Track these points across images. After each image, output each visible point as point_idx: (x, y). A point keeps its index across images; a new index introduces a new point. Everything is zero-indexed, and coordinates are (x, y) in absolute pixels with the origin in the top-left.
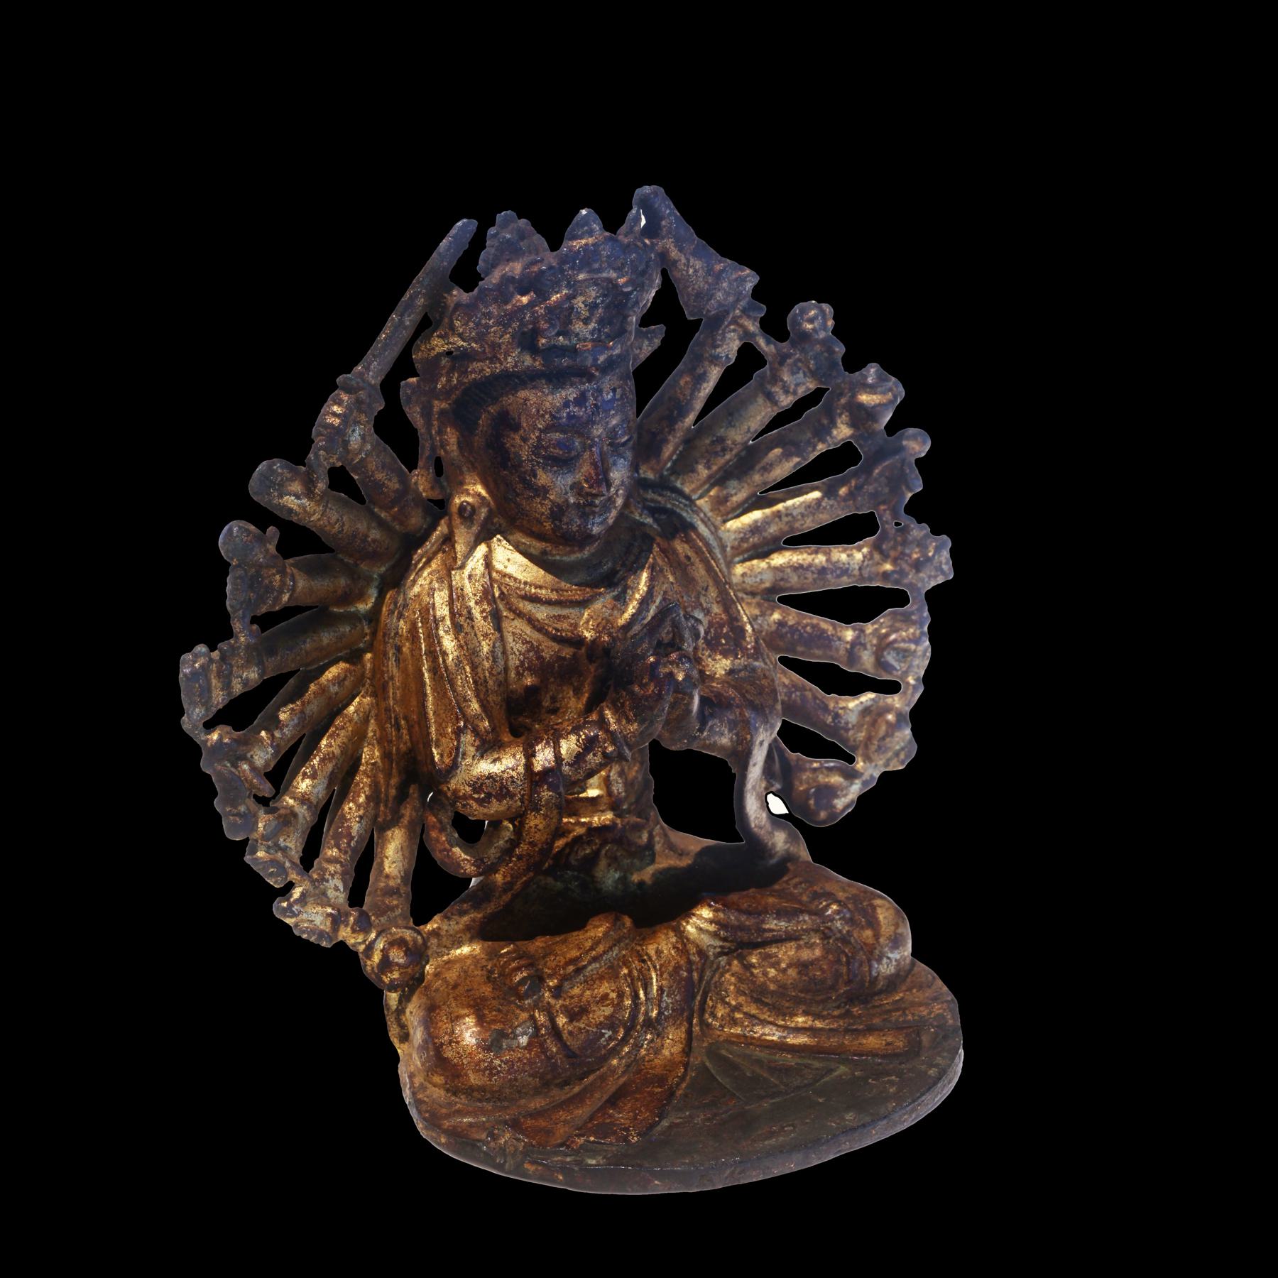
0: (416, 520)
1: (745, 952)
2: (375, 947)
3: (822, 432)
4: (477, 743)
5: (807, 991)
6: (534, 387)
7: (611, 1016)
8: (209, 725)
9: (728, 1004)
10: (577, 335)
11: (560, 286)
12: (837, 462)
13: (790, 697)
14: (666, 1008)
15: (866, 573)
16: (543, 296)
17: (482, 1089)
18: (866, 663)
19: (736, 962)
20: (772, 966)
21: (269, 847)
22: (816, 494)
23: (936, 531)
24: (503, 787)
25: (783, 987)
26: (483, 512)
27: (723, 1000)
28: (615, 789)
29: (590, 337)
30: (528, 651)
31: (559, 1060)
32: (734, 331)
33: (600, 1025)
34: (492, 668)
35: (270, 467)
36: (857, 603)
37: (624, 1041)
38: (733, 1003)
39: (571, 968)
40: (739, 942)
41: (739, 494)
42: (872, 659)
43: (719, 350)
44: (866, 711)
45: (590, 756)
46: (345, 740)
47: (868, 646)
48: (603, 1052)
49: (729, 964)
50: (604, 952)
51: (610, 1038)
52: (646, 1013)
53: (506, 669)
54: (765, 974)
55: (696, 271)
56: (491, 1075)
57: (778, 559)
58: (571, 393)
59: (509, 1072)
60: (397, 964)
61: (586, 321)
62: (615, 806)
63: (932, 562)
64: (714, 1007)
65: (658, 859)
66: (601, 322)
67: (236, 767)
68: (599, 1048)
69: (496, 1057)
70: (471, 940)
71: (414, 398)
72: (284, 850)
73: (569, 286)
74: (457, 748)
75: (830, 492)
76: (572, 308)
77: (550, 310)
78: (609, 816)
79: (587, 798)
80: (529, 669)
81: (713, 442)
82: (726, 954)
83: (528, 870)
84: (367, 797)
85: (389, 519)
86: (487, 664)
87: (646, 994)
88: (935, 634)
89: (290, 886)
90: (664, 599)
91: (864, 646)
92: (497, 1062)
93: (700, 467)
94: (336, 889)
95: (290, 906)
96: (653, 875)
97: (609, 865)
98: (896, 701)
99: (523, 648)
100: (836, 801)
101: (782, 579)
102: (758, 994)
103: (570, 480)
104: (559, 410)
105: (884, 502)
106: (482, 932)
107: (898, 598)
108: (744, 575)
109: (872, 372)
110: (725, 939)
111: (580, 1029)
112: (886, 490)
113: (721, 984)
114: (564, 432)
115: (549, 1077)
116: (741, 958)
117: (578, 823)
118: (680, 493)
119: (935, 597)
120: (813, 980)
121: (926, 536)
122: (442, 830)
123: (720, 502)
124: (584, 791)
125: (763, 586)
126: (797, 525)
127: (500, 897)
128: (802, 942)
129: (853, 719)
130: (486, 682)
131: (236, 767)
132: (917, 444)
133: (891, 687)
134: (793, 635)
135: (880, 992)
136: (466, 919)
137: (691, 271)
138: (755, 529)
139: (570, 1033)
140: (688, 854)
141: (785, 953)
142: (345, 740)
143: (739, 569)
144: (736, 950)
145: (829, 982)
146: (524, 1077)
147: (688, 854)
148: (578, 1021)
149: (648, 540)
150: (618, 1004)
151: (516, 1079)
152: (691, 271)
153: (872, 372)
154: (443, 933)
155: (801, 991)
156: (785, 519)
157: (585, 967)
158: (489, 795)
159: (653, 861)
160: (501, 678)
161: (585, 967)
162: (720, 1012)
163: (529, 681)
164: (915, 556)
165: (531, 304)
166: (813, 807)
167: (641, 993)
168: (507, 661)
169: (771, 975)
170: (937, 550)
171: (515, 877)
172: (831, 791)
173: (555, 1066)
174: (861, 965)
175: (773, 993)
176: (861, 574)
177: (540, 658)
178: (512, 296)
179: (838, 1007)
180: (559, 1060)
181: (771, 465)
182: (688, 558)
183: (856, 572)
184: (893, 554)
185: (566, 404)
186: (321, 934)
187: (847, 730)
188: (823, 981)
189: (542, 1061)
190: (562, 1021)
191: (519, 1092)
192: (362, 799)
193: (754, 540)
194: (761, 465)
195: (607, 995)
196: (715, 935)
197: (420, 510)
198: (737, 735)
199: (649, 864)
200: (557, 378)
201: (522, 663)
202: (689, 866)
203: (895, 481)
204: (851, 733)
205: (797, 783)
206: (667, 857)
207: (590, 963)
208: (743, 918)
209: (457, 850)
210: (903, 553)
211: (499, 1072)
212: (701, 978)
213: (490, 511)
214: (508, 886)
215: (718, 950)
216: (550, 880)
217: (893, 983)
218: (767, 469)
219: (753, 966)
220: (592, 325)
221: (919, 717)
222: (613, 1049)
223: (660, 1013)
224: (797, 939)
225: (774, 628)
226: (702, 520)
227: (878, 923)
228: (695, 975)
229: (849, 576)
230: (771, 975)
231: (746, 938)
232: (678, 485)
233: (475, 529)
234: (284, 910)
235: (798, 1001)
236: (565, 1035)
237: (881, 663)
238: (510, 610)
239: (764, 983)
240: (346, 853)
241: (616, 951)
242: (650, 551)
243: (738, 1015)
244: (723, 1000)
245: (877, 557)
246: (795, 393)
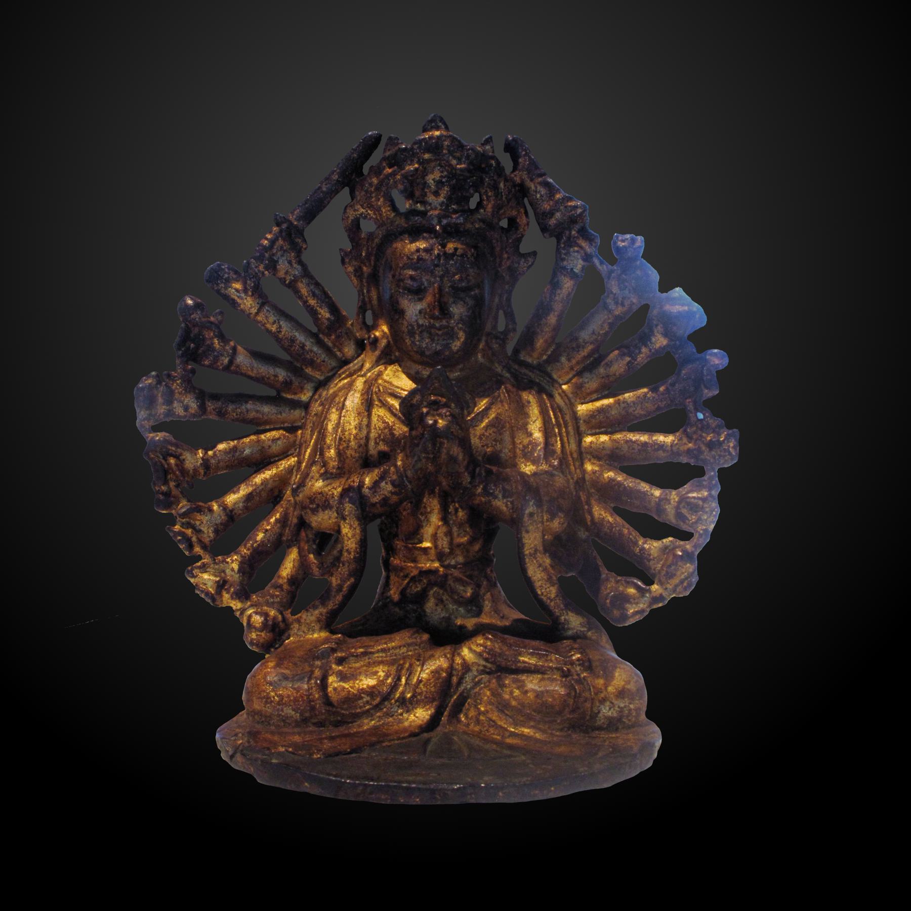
0: (349, 350)
1: (503, 675)
2: (253, 616)
3: (645, 339)
4: (322, 471)
5: (539, 712)
6: (402, 240)
7: (374, 687)
8: (155, 429)
9: (479, 709)
10: (430, 204)
11: (412, 161)
12: (660, 369)
13: (611, 530)
14: (420, 694)
15: (675, 449)
16: (401, 168)
17: (259, 713)
18: (670, 516)
19: (494, 681)
20: (518, 688)
21: (183, 524)
22: (645, 390)
23: (729, 427)
24: (327, 500)
25: (523, 705)
26: (383, 343)
27: (476, 706)
28: (440, 543)
29: (439, 207)
30: (385, 428)
31: (318, 705)
32: (577, 252)
33: (362, 691)
34: (357, 434)
35: (219, 266)
36: (672, 474)
37: (377, 707)
38: (482, 709)
39: (361, 650)
40: (500, 668)
41: (592, 383)
42: (673, 512)
43: (565, 263)
44: (665, 549)
45: (383, 484)
46: (268, 477)
47: (672, 502)
48: (359, 710)
49: (489, 681)
50: (393, 648)
51: (367, 702)
52: (403, 693)
53: (367, 438)
54: (511, 693)
55: (541, 196)
56: (266, 702)
57: (618, 436)
58: (422, 245)
59: (279, 703)
60: (255, 627)
61: (436, 194)
62: (440, 557)
63: (727, 449)
64: (468, 710)
65: (483, 615)
66: (449, 199)
67: (166, 460)
68: (356, 707)
69: (273, 690)
70: (321, 629)
71: (347, 260)
72: (198, 531)
73: (418, 162)
74: (308, 475)
75: (654, 390)
76: (425, 183)
77: (405, 177)
78: (436, 565)
79: (421, 548)
80: (383, 440)
81: (571, 341)
82: (488, 673)
83: (350, 575)
84: (276, 519)
85: (330, 344)
86: (354, 432)
87: (407, 680)
88: (721, 499)
89: (199, 558)
90: (496, 418)
91: (668, 501)
92: (273, 694)
93: (563, 359)
94: (233, 570)
95: (192, 570)
96: (475, 625)
97: (437, 605)
98: (688, 546)
99: (382, 426)
100: (628, 605)
101: (617, 448)
102: (503, 707)
103: (419, 307)
104: (412, 253)
105: (690, 397)
106: (329, 624)
107: (698, 472)
108: (591, 443)
109: (678, 292)
110: (486, 660)
111: (344, 688)
112: (692, 389)
113: (480, 694)
114: (415, 269)
115: (307, 715)
116: (499, 678)
117: (416, 568)
118: (550, 377)
119: (723, 474)
120: (544, 704)
121: (719, 426)
122: (308, 541)
123: (579, 388)
124: (421, 542)
125: (604, 452)
126: (631, 410)
127: (335, 596)
128: (546, 676)
129: (654, 553)
130: (349, 441)
131: (166, 460)
132: (717, 358)
133: (686, 536)
134: (619, 487)
135: (600, 728)
136: (317, 612)
137: (538, 196)
138: (601, 410)
139: (335, 689)
140: (507, 619)
141: (533, 684)
142: (268, 477)
143: (588, 439)
144: (496, 672)
145: (557, 708)
146: (289, 711)
147: (507, 619)
148: (345, 682)
149: (499, 383)
150: (382, 681)
151: (282, 710)
152: (538, 196)
153: (678, 292)
154: (303, 621)
155: (535, 711)
156: (623, 405)
157: (373, 653)
158: (318, 506)
159: (478, 614)
160: (363, 442)
161: (373, 653)
162: (472, 713)
163: (382, 447)
164: (709, 438)
165: (394, 174)
166: (608, 605)
167: (403, 680)
168: (369, 432)
169: (515, 694)
170: (728, 437)
171: (344, 581)
172: (626, 599)
173: (313, 708)
174: (585, 701)
175: (513, 708)
176: (672, 450)
177: (392, 434)
178: (384, 169)
179: (561, 730)
180: (318, 705)
181: (611, 362)
182: (529, 402)
183: (669, 448)
184: (695, 437)
185: (418, 250)
186: (207, 593)
187: (649, 560)
188: (552, 706)
189: (303, 700)
190: (331, 679)
191: (284, 721)
192: (272, 520)
193: (601, 417)
194: (606, 361)
195: (378, 672)
196: (480, 655)
197: (352, 343)
198: (512, 503)
199: (473, 617)
200: (415, 233)
201: (380, 436)
202: (506, 626)
203: (699, 382)
204: (652, 563)
205: (603, 588)
206: (491, 617)
207: (378, 651)
208: (505, 648)
209: (312, 556)
210: (701, 436)
211: (272, 702)
212: (460, 683)
213: (389, 342)
214: (340, 588)
215: (481, 668)
216: (397, 610)
217: (613, 725)
218: (608, 365)
219: (504, 686)
220: (441, 199)
221: (705, 559)
222: (368, 711)
223: (413, 696)
224: (543, 673)
225: (607, 480)
226: (559, 394)
227: (613, 677)
228: (455, 679)
229: (664, 451)
230: (515, 694)
231: (503, 664)
232: (549, 369)
233: (377, 353)
234: (188, 571)
235: (529, 718)
236: (330, 689)
237: (679, 516)
238: (380, 401)
239: (509, 700)
240: (248, 549)
241: (404, 650)
242: (499, 388)
243: (482, 718)
244: (476, 706)
245: (685, 440)
246: (623, 305)
